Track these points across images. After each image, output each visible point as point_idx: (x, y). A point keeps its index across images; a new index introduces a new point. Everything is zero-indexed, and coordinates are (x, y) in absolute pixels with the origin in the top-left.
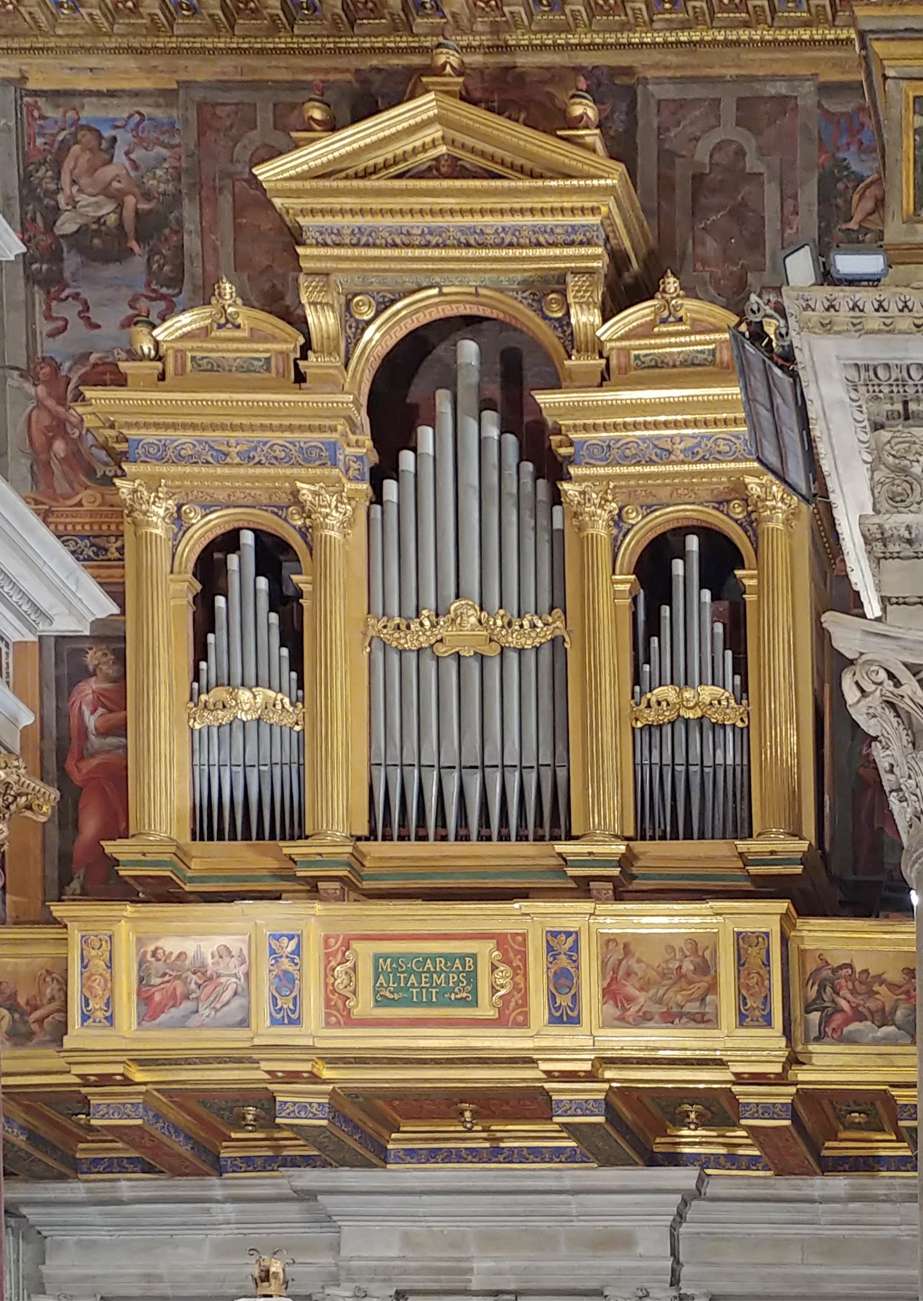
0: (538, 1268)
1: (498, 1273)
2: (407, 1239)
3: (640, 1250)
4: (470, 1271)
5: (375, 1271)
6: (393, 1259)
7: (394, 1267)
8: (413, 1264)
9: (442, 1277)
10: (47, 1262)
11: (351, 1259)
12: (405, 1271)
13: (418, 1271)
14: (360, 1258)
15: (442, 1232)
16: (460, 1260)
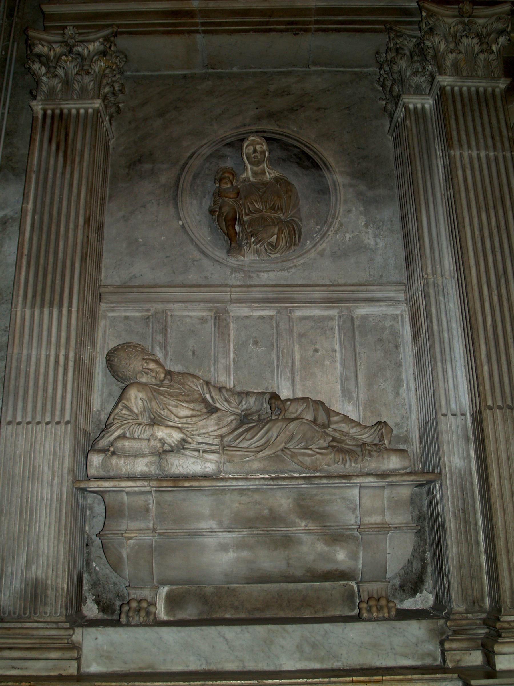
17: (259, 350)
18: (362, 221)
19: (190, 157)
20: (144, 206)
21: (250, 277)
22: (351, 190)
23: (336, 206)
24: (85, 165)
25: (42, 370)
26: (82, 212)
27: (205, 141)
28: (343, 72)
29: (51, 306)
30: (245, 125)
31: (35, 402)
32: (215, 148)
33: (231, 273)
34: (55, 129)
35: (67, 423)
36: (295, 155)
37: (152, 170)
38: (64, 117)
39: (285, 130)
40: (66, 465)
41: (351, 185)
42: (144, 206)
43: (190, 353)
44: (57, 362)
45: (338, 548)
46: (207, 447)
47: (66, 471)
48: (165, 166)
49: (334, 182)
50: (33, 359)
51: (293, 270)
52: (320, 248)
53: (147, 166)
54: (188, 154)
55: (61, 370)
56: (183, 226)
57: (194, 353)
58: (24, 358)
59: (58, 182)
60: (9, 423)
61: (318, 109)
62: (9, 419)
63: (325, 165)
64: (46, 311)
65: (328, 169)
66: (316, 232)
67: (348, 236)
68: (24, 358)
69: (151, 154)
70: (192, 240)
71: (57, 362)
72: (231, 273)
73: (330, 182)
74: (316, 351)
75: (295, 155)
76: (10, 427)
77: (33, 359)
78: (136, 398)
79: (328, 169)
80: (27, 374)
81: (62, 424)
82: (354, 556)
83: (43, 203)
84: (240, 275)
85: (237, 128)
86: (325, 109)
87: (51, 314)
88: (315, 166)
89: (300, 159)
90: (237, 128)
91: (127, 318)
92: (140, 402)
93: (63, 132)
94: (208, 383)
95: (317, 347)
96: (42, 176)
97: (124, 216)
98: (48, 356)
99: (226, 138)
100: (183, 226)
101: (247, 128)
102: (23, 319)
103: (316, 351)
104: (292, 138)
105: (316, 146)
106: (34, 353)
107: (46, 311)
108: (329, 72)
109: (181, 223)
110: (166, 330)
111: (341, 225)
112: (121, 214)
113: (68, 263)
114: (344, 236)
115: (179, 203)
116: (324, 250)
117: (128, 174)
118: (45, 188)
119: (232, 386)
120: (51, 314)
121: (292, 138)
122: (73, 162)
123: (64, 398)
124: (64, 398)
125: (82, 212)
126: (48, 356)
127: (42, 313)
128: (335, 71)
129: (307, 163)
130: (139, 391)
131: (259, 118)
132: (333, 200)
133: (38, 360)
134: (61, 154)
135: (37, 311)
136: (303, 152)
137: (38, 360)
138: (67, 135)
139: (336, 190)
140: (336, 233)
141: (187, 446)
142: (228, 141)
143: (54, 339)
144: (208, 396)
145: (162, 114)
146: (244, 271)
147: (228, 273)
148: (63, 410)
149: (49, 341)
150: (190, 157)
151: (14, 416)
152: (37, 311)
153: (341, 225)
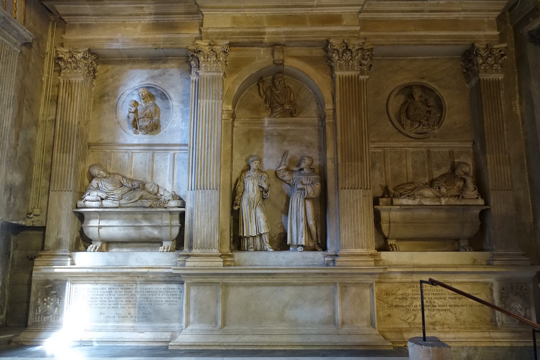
0: (296, 32)
1: (278, 33)
2: (235, 20)
3: (344, 23)
4: (264, 33)
5: (219, 34)
6: (228, 28)
7: (228, 32)
8: (238, 31)
9: (250, 36)
10: (66, 34)
11: (208, 28)
12: (234, 34)
13: (239, 34)
14: (213, 28)
15: (251, 16)
16: (260, 28)
17: (142, 166)
18: (181, 120)
19: (122, 95)
20: (105, 114)
21: (140, 140)
22: (178, 108)
23: (172, 114)
24: (78, 102)
25: (63, 174)
26: (77, 120)
27: (128, 88)
28: (180, 59)
29: (66, 153)
30: (142, 82)
31: (60, 184)
32: (131, 91)
33: (134, 139)
34: (68, 88)
35: (71, 191)
36: (160, 94)
37: (108, 99)
38: (71, 83)
39: (157, 84)
40: (70, 204)
41: (178, 106)
42: (105, 114)
43: (119, 166)
44: (68, 171)
45: (155, 231)
46: (114, 199)
47: (70, 206)
48: (112, 98)
49: (172, 105)
50: (60, 170)
51: (155, 138)
52: (165, 130)
53: (106, 98)
54: (121, 94)
55: (69, 174)
56: (118, 121)
57: (120, 166)
58: (57, 170)
59: (69, 109)
60: (53, 191)
61: (170, 75)
62: (52, 189)
63: (170, 98)
64: (65, 154)
65: (171, 99)
66: (164, 124)
67: (175, 125)
68: (57, 170)
69: (108, 93)
70: (121, 126)
71: (68, 171)
72: (134, 139)
73: (171, 105)
74: (161, 166)
75: (160, 94)
76: (53, 192)
77: (60, 170)
78: (95, 183)
79: (171, 99)
80: (58, 175)
81: (69, 191)
82: (160, 233)
83: (64, 116)
84: (137, 140)
85: (140, 83)
86: (172, 75)
87: (66, 155)
88: (167, 99)
89: (161, 95)
90: (140, 83)
91: (98, 154)
92: (96, 185)
93: (70, 89)
94: (123, 177)
95: (162, 165)
96: (63, 106)
97: (97, 117)
98: (65, 170)
99: (135, 87)
100: (118, 121)
101: (143, 83)
102: (57, 157)
103: (161, 166)
104: (159, 87)
105: (168, 90)
106: (61, 168)
107: (65, 154)
108: (175, 59)
109: (117, 120)
110: (111, 159)
111: (173, 121)
112: (96, 116)
113: (72, 138)
114: (174, 125)
115: (117, 113)
116: (166, 131)
117: (99, 101)
118: (64, 111)
119: (132, 178)
120: (66, 155)
121: (159, 87)
122: (74, 101)
123: (70, 183)
124: (70, 183)
125: (77, 120)
126: (65, 170)
127: (63, 156)
128: (178, 59)
129: (164, 97)
130: (96, 181)
131: (148, 79)
132: (171, 112)
133: (62, 171)
134: (70, 98)
135: (62, 155)
136: (163, 93)
137: (62, 171)
138: (72, 90)
139: (173, 108)
140: (171, 124)
141: (108, 198)
142: (136, 88)
143: (67, 164)
144: (122, 182)
145: (112, 77)
146: (138, 138)
147: (133, 138)
148: (70, 187)
149: (65, 165)
150: (122, 95)
151: (54, 188)
152: (62, 155)
153: (173, 121)
